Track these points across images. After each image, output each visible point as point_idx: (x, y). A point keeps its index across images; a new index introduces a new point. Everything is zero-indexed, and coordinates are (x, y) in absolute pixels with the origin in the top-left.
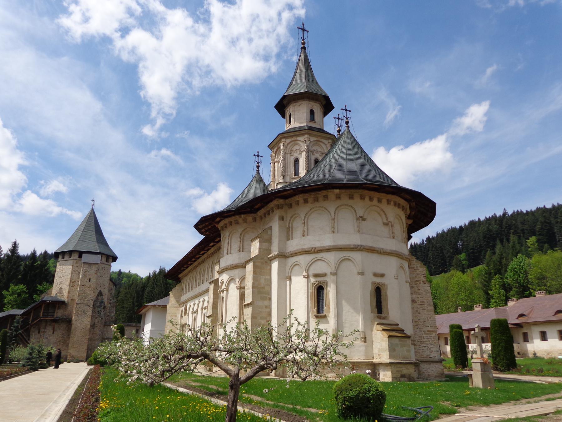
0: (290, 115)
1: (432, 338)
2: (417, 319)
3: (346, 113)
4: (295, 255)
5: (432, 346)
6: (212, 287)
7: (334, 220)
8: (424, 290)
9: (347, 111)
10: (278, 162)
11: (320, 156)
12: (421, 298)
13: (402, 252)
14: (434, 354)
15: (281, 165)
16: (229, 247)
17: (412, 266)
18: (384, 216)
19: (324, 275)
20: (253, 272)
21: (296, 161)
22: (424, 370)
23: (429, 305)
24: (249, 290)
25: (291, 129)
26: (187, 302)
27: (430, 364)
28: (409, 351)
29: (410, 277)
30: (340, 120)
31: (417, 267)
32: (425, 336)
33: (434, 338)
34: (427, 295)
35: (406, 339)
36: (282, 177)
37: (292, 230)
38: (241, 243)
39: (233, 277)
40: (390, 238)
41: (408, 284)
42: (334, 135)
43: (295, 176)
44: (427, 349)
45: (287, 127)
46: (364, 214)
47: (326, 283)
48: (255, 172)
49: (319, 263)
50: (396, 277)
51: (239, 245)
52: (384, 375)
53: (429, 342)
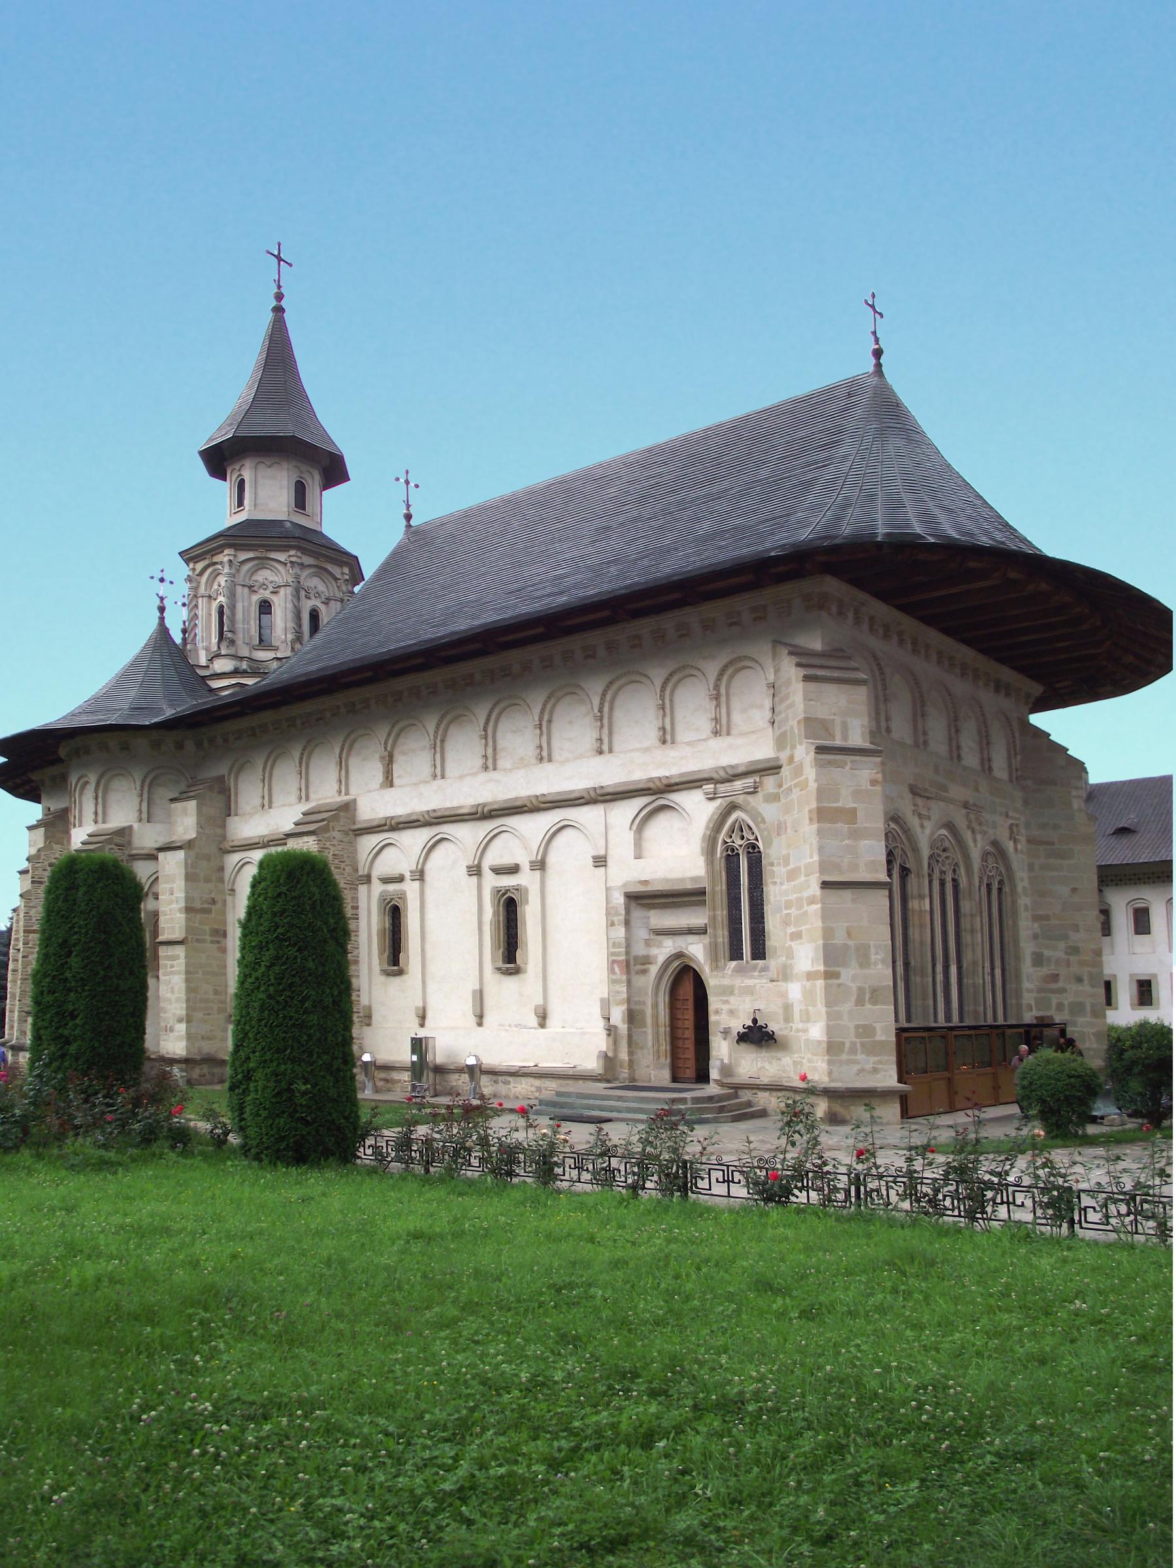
25: (248, 523)
48: (157, 621)
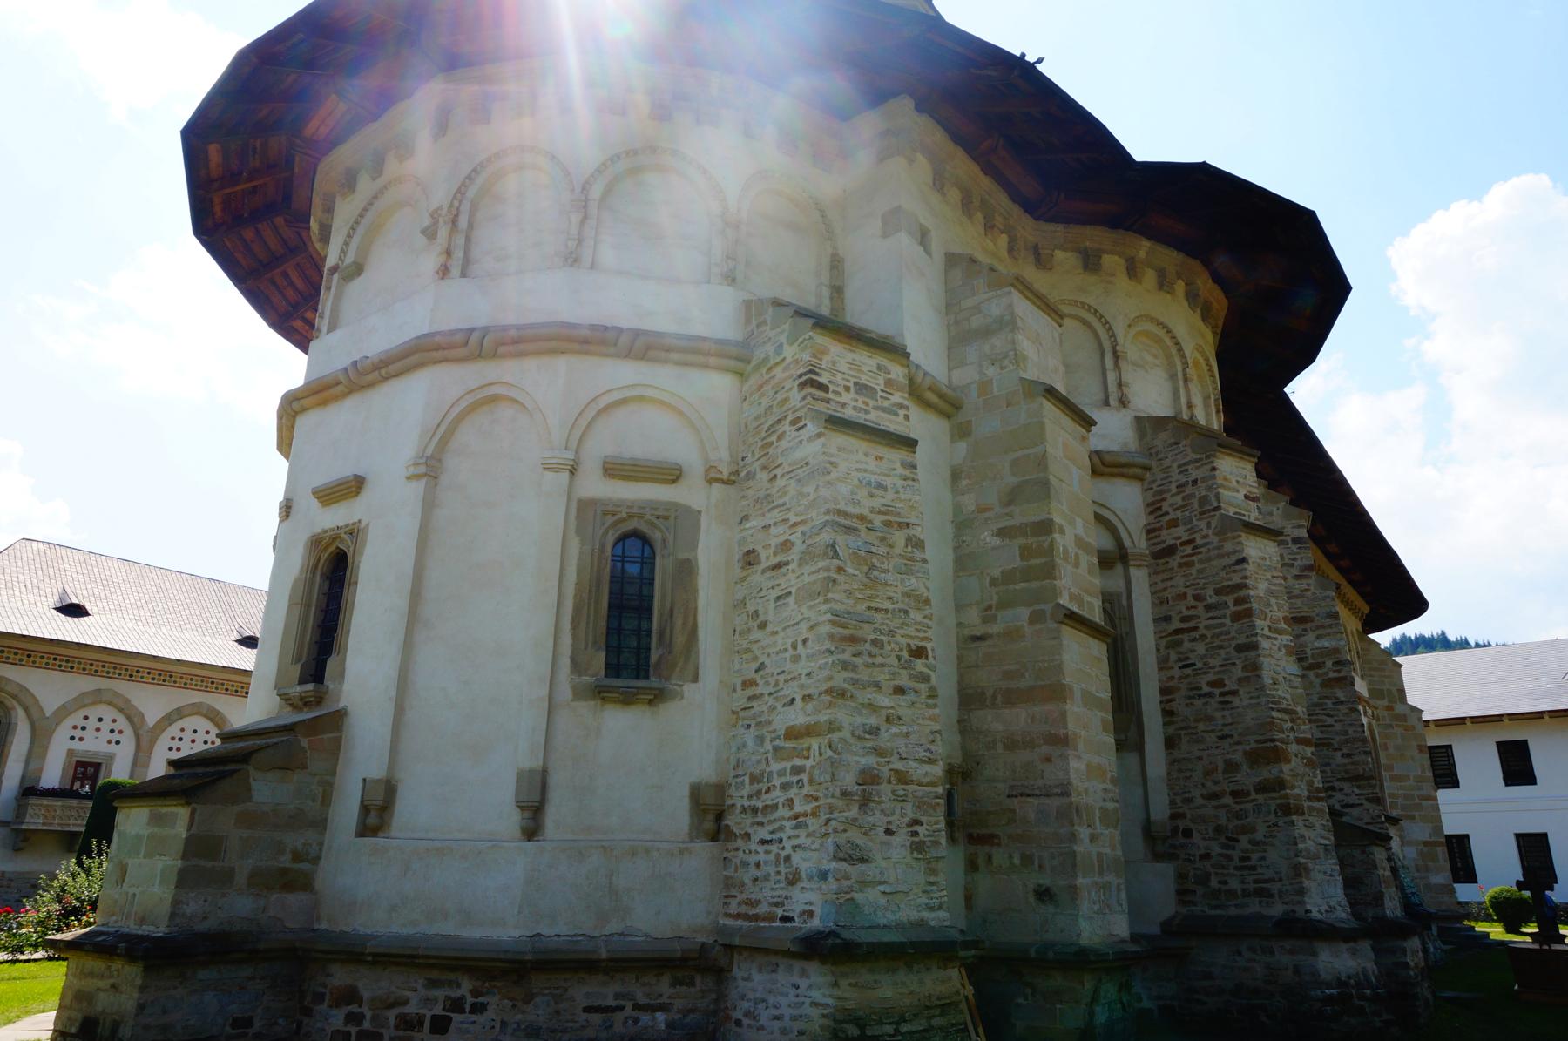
1: (804, 777)
2: (755, 666)
34: (801, 494)
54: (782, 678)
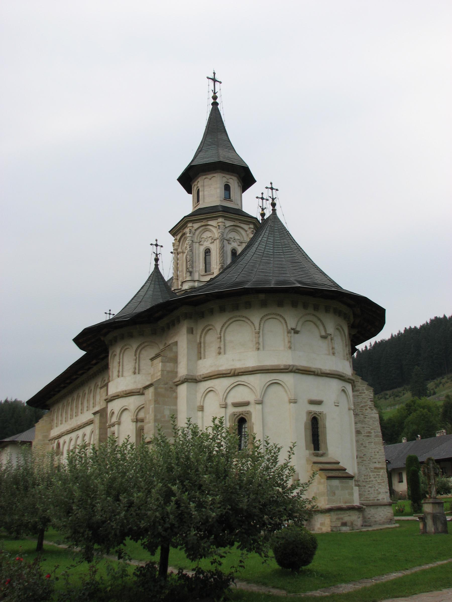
0: (199, 189)
1: (380, 476)
2: (363, 454)
3: (272, 192)
4: (209, 378)
5: (380, 486)
6: (97, 419)
7: (259, 333)
8: (371, 418)
9: (274, 190)
10: (183, 253)
11: (239, 245)
12: (368, 429)
13: (345, 372)
14: (382, 496)
15: (186, 258)
16: (121, 367)
17: (357, 388)
18: (321, 327)
19: (247, 404)
20: (155, 401)
21: (207, 252)
22: (370, 515)
23: (377, 436)
24: (150, 425)
26: (59, 437)
27: (377, 508)
28: (351, 494)
29: (354, 403)
30: (264, 201)
31: (363, 390)
32: (371, 474)
33: (382, 477)
35: (348, 480)
36: (188, 274)
37: (205, 346)
38: (136, 363)
39: (127, 407)
40: (329, 355)
41: (352, 412)
42: (256, 218)
43: (206, 272)
44: (374, 490)
45: (195, 206)
46: (297, 325)
47: (249, 413)
49: (241, 388)
50: (336, 404)
51: (133, 364)
52: (322, 524)
53: (376, 480)
54: (372, 458)
